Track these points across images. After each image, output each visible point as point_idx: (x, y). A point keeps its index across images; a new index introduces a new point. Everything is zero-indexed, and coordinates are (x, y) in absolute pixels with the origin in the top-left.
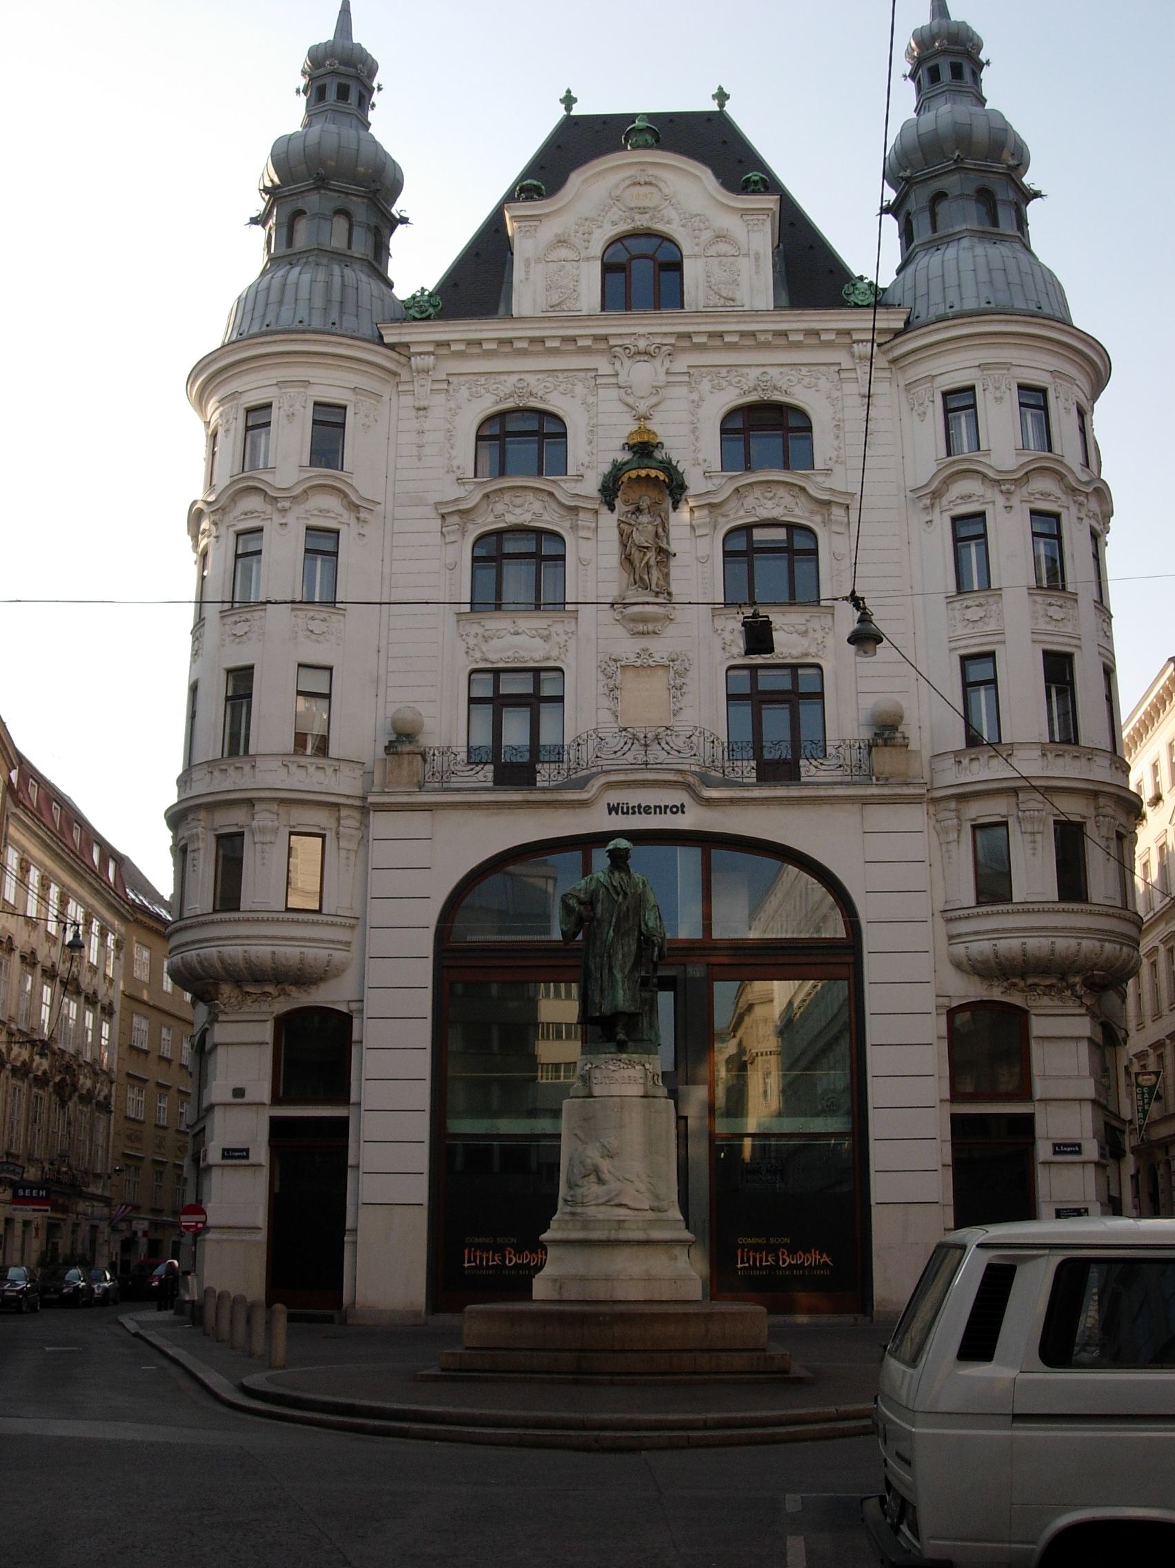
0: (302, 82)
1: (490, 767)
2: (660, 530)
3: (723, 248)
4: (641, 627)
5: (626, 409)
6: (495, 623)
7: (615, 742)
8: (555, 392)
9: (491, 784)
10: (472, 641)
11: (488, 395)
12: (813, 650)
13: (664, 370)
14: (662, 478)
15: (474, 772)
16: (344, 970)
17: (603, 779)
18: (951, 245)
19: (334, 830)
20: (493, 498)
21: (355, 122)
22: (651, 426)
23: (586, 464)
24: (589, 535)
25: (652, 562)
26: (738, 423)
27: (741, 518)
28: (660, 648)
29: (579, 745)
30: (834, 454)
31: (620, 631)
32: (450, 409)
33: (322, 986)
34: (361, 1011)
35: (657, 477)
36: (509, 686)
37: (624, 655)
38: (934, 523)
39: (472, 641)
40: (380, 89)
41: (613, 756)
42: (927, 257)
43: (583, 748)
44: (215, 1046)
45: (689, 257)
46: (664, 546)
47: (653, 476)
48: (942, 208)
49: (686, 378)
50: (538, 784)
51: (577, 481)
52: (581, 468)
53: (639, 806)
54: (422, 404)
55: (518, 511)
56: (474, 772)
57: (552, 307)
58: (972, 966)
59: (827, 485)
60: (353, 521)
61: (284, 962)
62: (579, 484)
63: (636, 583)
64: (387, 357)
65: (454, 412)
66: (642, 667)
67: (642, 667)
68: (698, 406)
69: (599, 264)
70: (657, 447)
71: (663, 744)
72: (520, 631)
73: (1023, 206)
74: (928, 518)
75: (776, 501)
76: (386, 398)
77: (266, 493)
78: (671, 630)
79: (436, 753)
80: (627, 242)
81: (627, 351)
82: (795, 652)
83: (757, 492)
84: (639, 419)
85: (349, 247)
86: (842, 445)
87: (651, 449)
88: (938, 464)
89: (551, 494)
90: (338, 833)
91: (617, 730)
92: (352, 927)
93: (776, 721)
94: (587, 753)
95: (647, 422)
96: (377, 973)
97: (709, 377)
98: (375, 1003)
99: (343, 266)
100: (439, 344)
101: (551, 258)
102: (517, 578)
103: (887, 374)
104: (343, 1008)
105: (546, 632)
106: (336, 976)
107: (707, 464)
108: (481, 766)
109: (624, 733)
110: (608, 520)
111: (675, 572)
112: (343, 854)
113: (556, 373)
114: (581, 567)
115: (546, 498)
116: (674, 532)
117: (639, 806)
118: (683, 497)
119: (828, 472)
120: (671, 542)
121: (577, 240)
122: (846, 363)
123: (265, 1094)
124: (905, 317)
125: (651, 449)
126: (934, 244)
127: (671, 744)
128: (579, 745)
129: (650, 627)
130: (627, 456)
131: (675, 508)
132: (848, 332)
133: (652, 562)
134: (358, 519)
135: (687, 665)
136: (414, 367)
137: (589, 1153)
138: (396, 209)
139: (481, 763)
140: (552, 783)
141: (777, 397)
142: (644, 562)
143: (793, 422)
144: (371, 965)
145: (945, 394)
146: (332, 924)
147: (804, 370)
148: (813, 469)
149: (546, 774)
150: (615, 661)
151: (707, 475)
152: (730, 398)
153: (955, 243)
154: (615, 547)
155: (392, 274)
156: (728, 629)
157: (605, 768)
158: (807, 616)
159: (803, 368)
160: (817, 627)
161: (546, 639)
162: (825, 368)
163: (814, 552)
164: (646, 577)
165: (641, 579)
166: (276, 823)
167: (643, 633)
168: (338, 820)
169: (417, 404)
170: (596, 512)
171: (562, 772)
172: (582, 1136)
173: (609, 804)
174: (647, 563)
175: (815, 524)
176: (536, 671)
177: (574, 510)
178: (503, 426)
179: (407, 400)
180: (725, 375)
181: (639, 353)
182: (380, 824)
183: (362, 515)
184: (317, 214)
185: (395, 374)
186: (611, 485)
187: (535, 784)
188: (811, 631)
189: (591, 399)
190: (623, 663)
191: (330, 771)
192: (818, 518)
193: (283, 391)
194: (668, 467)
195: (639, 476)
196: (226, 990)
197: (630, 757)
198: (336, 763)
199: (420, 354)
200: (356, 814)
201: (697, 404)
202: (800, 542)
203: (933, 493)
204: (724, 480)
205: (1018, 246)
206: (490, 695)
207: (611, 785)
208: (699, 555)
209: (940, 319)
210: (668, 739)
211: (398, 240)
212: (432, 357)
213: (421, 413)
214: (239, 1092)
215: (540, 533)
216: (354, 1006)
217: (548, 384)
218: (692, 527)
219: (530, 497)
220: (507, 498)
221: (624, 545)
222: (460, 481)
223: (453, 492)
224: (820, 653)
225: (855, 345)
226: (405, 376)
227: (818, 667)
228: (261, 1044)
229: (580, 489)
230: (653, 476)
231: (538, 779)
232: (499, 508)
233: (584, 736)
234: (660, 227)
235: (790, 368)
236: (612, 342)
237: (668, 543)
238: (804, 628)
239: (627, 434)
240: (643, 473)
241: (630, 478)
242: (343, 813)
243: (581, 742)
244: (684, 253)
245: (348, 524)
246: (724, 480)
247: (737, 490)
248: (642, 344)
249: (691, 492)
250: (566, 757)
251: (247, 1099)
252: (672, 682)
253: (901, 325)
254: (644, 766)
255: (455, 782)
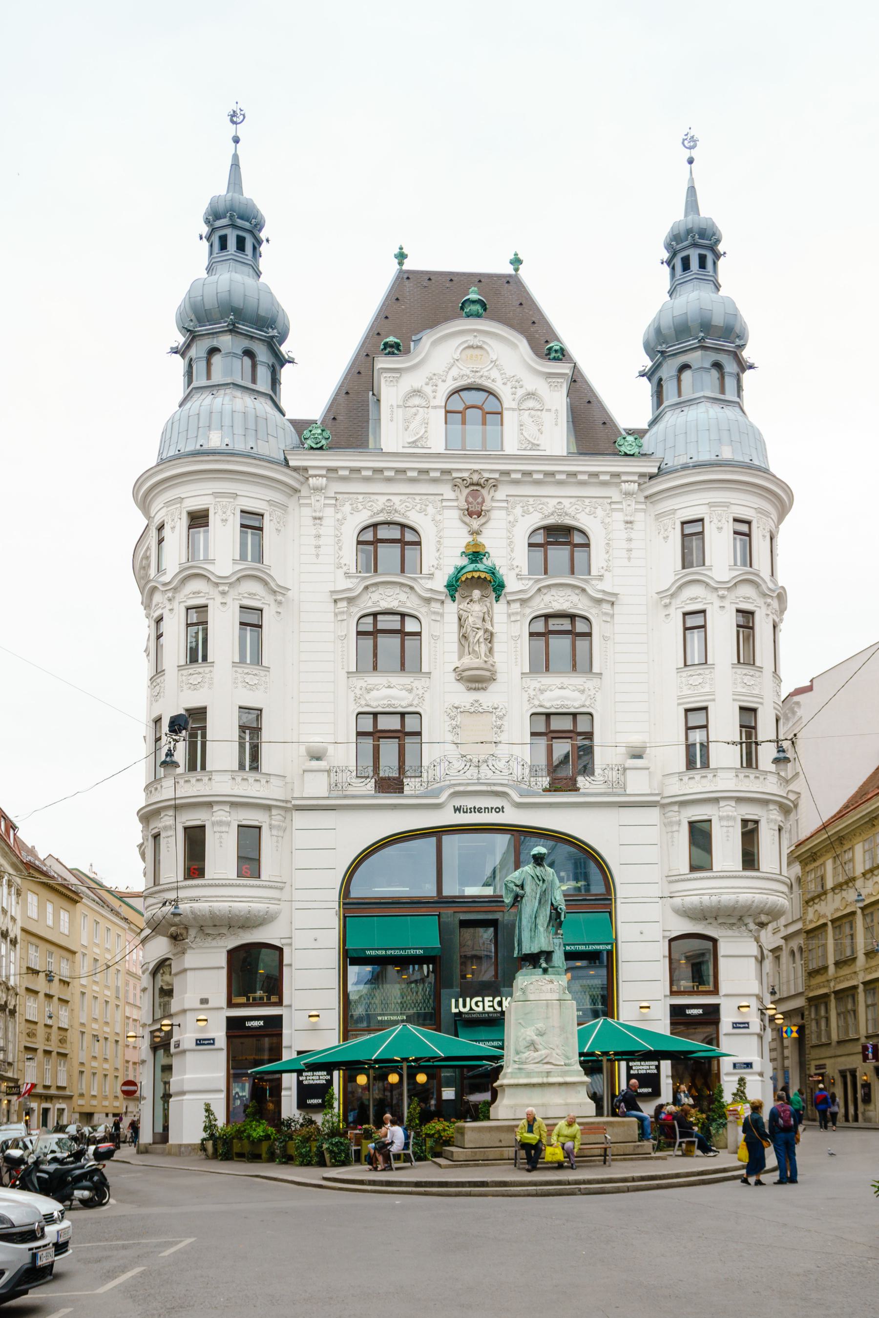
0: (205, 230)
1: (373, 780)
2: (486, 616)
3: (531, 403)
4: (473, 685)
5: (463, 525)
6: (374, 680)
7: (458, 765)
8: (413, 510)
9: (373, 792)
10: (358, 692)
11: (365, 510)
12: (587, 703)
13: (490, 496)
14: (489, 579)
15: (364, 784)
16: (276, 918)
17: (452, 790)
18: (692, 407)
19: (268, 823)
20: (371, 589)
21: (251, 271)
22: (481, 539)
23: (436, 566)
24: (438, 618)
25: (481, 640)
26: (540, 538)
27: (543, 609)
28: (488, 698)
29: (434, 766)
30: (605, 565)
31: (460, 687)
32: (338, 520)
33: (261, 928)
34: (291, 945)
35: (485, 578)
36: (386, 723)
37: (463, 704)
38: (671, 616)
39: (358, 692)
40: (268, 241)
41: (458, 774)
42: (675, 416)
43: (438, 768)
44: (185, 970)
45: (508, 409)
46: (490, 628)
47: (483, 577)
48: (687, 375)
49: (505, 504)
50: (405, 792)
51: (429, 578)
52: (433, 569)
53: (475, 808)
54: (318, 514)
55: (389, 599)
56: (364, 784)
57: (409, 443)
58: (685, 911)
59: (599, 587)
60: (272, 603)
61: (237, 913)
62: (430, 582)
63: (470, 654)
64: (295, 478)
65: (341, 522)
66: (475, 712)
67: (475, 712)
68: (514, 526)
69: (443, 411)
70: (485, 556)
71: (491, 767)
72: (392, 686)
73: (741, 374)
74: (667, 613)
75: (566, 598)
76: (290, 509)
77: (209, 579)
78: (493, 687)
79: (338, 770)
80: (463, 394)
81: (465, 482)
82: (576, 704)
83: (553, 591)
84: (472, 534)
85: (254, 381)
86: (610, 558)
87: (482, 557)
88: (675, 575)
89: (412, 588)
90: (270, 825)
91: (460, 756)
92: (281, 889)
93: (562, 748)
94: (439, 772)
95: (478, 536)
96: (300, 920)
97: (521, 504)
98: (301, 939)
99: (252, 398)
100: (330, 470)
101: (409, 404)
102: (389, 645)
103: (643, 507)
104: (276, 943)
105: (410, 687)
106: (270, 922)
107: (519, 569)
108: (368, 780)
109: (464, 758)
110: (451, 609)
111: (497, 647)
112: (275, 838)
113: (414, 496)
114: (433, 641)
115: (407, 590)
116: (496, 618)
117: (475, 808)
118: (503, 592)
119: (601, 577)
120: (495, 625)
121: (428, 390)
122: (616, 497)
123: (223, 1001)
124: (658, 465)
125: (482, 557)
126: (679, 406)
127: (495, 766)
128: (434, 766)
129: (480, 686)
130: (465, 561)
131: (498, 599)
132: (617, 475)
133: (481, 640)
134: (276, 601)
135: (504, 712)
136: (311, 486)
137: (528, 1033)
138: (284, 349)
139: (368, 777)
140: (417, 792)
141: (568, 521)
142: (476, 639)
143: (578, 539)
144: (297, 914)
145: (683, 523)
146: (271, 887)
147: (587, 501)
148: (589, 574)
149: (411, 785)
150: (457, 708)
151: (519, 577)
152: (536, 520)
153: (695, 406)
154: (455, 627)
155: (283, 404)
156: (532, 687)
157: (452, 782)
158: (584, 679)
159: (585, 500)
160: (592, 688)
161: (410, 691)
162: (601, 500)
163: (589, 635)
164: (477, 649)
165: (473, 650)
166: (229, 819)
167: (475, 689)
168: (270, 816)
169: (314, 514)
170: (443, 602)
171: (423, 784)
172: (524, 1024)
173: (454, 806)
174: (478, 640)
175: (592, 613)
176: (403, 715)
177: (428, 601)
178: (375, 534)
179: (307, 512)
180: (533, 503)
181: (472, 484)
182: (300, 820)
183: (279, 598)
184: (230, 353)
185: (296, 491)
186: (454, 583)
187: (403, 792)
188: (587, 691)
189: (438, 517)
190: (462, 710)
191: (263, 781)
192: (594, 611)
193: (217, 500)
194: (493, 572)
195: (473, 577)
196: (192, 932)
197: (468, 774)
198: (268, 777)
199: (316, 476)
200: (282, 813)
201: (512, 524)
202: (581, 627)
203: (672, 595)
204: (531, 582)
205: (738, 409)
206: (371, 729)
207: (456, 794)
208: (513, 635)
209: (685, 467)
210: (494, 763)
211: (286, 372)
212: (325, 479)
213: (318, 521)
214: (204, 1001)
215: (403, 615)
216: (284, 941)
217: (407, 504)
218: (509, 615)
219: (397, 590)
220: (381, 590)
221: (461, 626)
222: (347, 575)
223: (343, 584)
224: (592, 705)
225: (623, 484)
226: (304, 492)
227: (591, 714)
228: (218, 968)
229: (429, 585)
230: (483, 577)
231: (406, 788)
232: (375, 596)
233: (438, 760)
234: (487, 384)
235: (577, 499)
236: (455, 475)
237: (492, 626)
238: (582, 688)
239: (465, 545)
240: (476, 575)
241: (467, 579)
242: (274, 812)
243: (436, 764)
244: (505, 405)
245: (269, 605)
246: (531, 582)
247: (539, 590)
248: (475, 478)
249: (507, 589)
250: (425, 775)
251: (210, 1005)
252: (495, 724)
253: (655, 470)
254: (476, 781)
255: (351, 791)
